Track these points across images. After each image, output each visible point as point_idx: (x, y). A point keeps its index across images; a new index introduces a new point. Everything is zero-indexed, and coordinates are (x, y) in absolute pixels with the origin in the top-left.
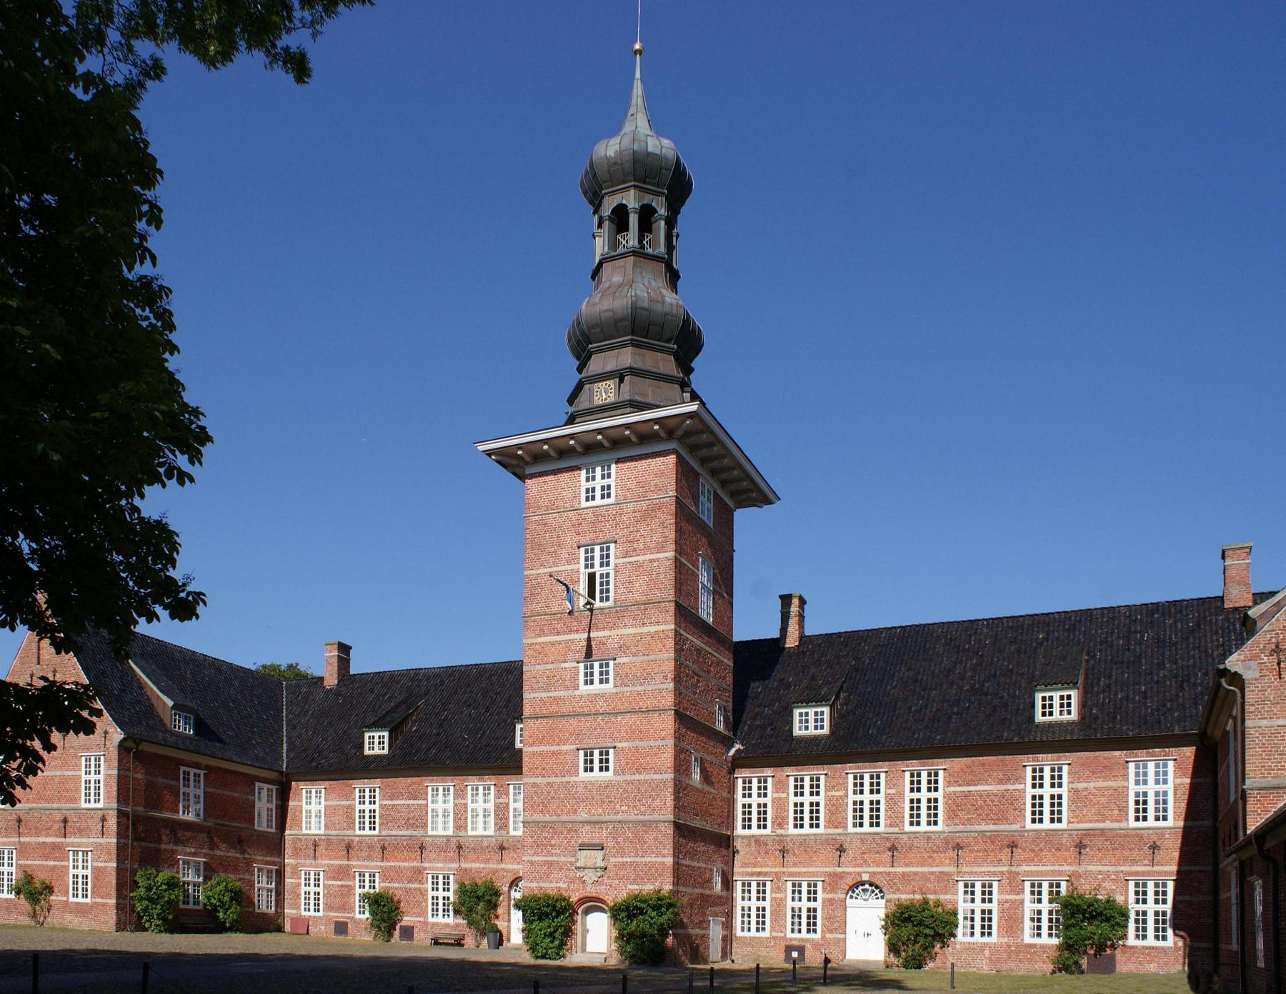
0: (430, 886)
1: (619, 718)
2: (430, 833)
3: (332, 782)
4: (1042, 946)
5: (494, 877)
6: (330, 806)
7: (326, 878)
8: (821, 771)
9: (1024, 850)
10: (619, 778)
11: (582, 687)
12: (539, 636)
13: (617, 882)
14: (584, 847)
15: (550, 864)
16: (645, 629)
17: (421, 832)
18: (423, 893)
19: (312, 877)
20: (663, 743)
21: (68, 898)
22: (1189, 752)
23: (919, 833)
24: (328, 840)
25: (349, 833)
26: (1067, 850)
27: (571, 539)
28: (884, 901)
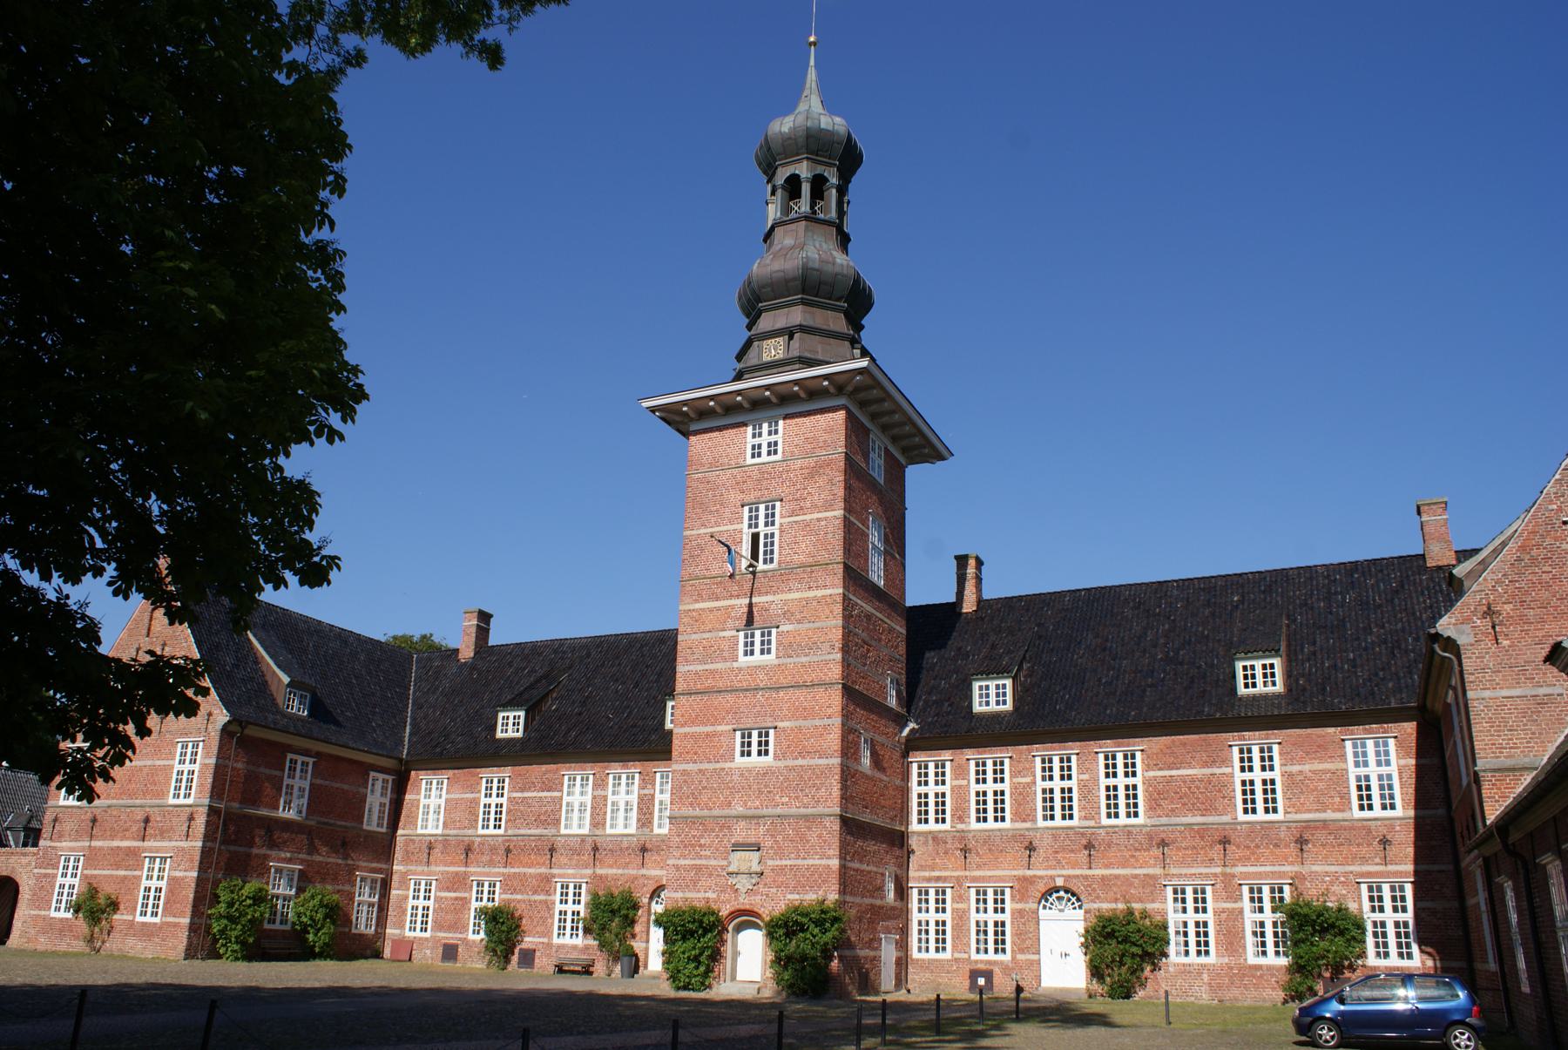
0: (558, 897)
1: (781, 694)
2: (563, 831)
3: (456, 771)
5: (632, 886)
6: (452, 800)
7: (439, 889)
8: (1004, 754)
9: (1238, 847)
12: (696, 601)
14: (738, 847)
15: (698, 868)
16: (811, 594)
17: (553, 831)
19: (423, 887)
21: (134, 917)
22: (1410, 728)
24: (445, 841)
26: (1287, 846)
27: (734, 497)
28: (1082, 911)
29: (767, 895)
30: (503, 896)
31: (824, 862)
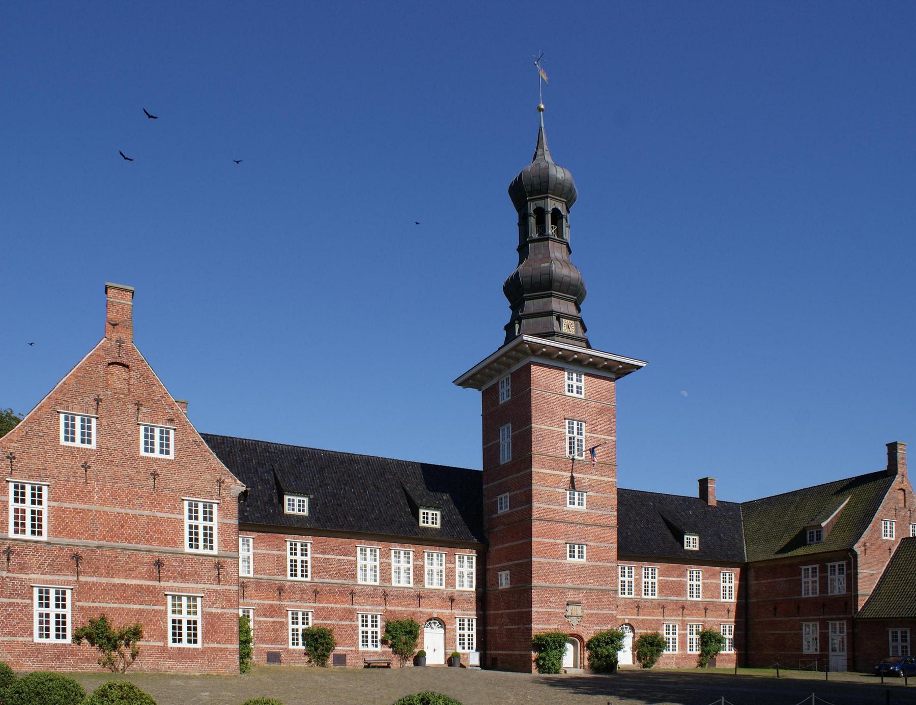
1: (589, 528)
5: (413, 617)
10: (589, 563)
11: (568, 505)
15: (550, 613)
16: (602, 478)
17: (352, 582)
18: (354, 629)
20: (612, 545)
25: (280, 578)
29: (585, 627)
30: (316, 621)
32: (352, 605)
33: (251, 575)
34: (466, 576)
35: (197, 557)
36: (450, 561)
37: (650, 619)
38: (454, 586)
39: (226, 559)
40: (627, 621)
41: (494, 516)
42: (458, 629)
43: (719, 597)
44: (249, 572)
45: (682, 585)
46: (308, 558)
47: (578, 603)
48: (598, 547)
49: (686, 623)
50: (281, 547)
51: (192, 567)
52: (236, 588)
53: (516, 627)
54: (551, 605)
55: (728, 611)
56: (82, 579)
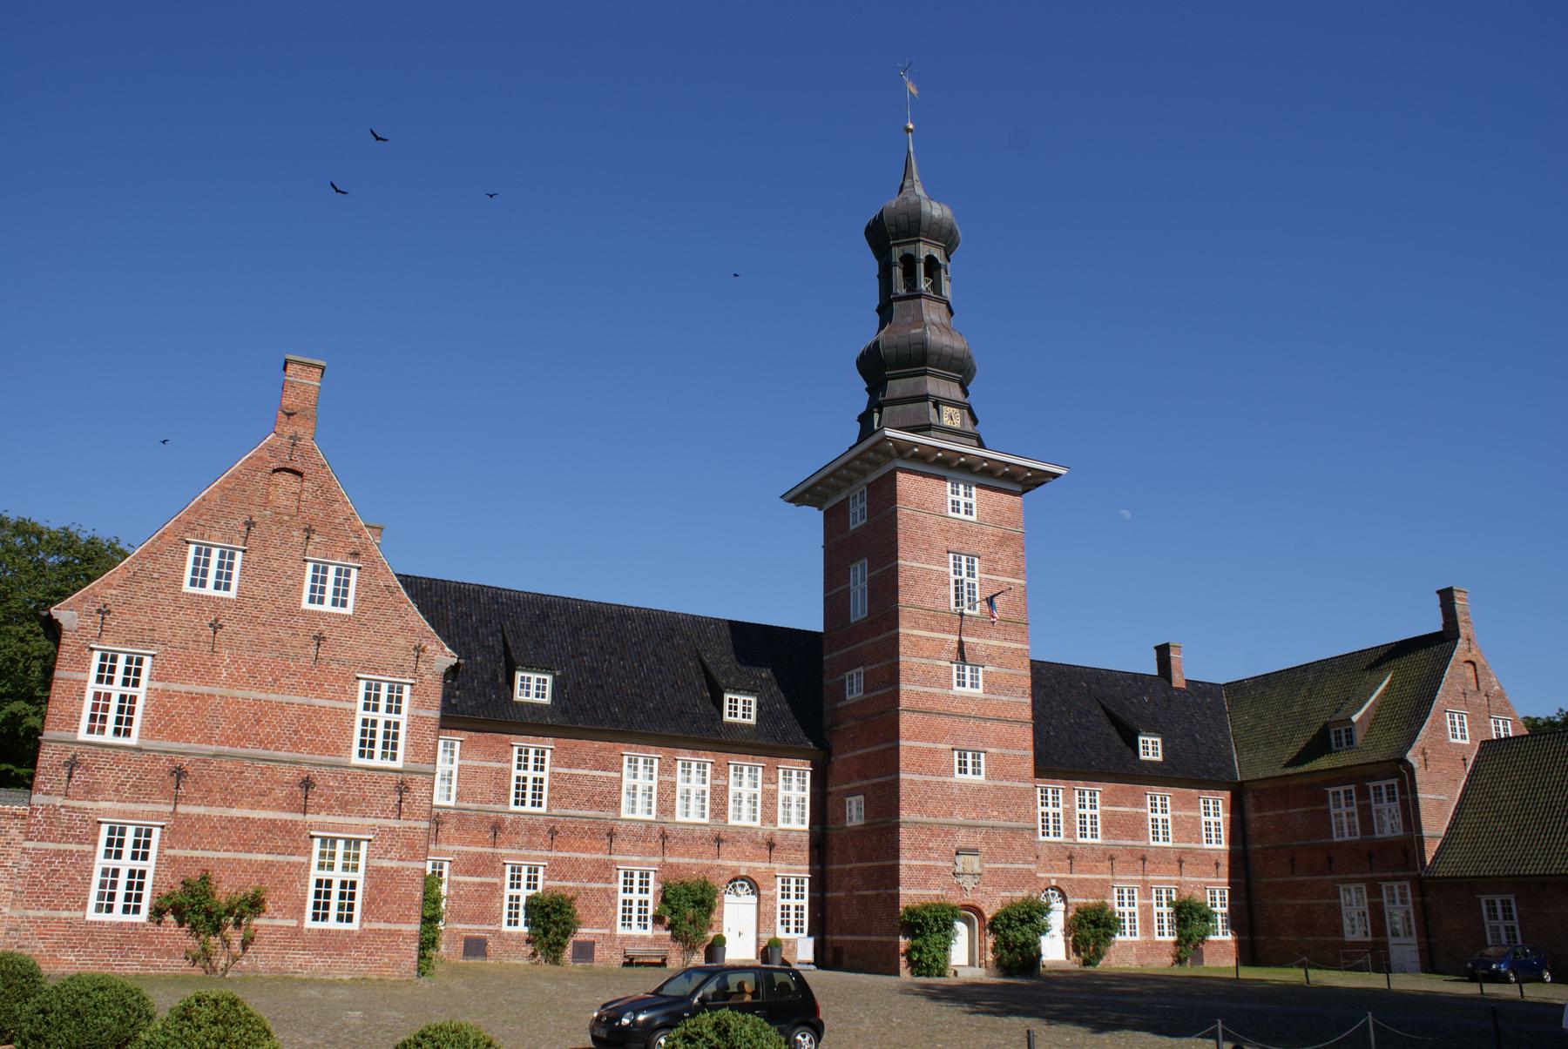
1: (988, 724)
4: (1166, 943)
5: (708, 876)
9: (1150, 862)
11: (956, 688)
13: (991, 889)
15: (928, 869)
16: (1007, 644)
17: (611, 814)
18: (610, 896)
20: (1023, 753)
23: (1087, 844)
25: (498, 807)
30: (549, 883)
31: (1026, 866)
32: (610, 854)
33: (452, 803)
34: (794, 803)
35: (370, 773)
36: (770, 779)
37: (1091, 879)
38: (774, 821)
39: (414, 776)
40: (1054, 883)
41: (840, 705)
42: (779, 896)
43: (1199, 841)
44: (449, 798)
45: (1140, 820)
46: (545, 775)
47: (974, 852)
48: (1003, 755)
49: (1150, 885)
50: (503, 756)
51: (360, 789)
52: (426, 825)
53: (874, 893)
54: (931, 855)
55: (1217, 864)
56: (182, 809)
